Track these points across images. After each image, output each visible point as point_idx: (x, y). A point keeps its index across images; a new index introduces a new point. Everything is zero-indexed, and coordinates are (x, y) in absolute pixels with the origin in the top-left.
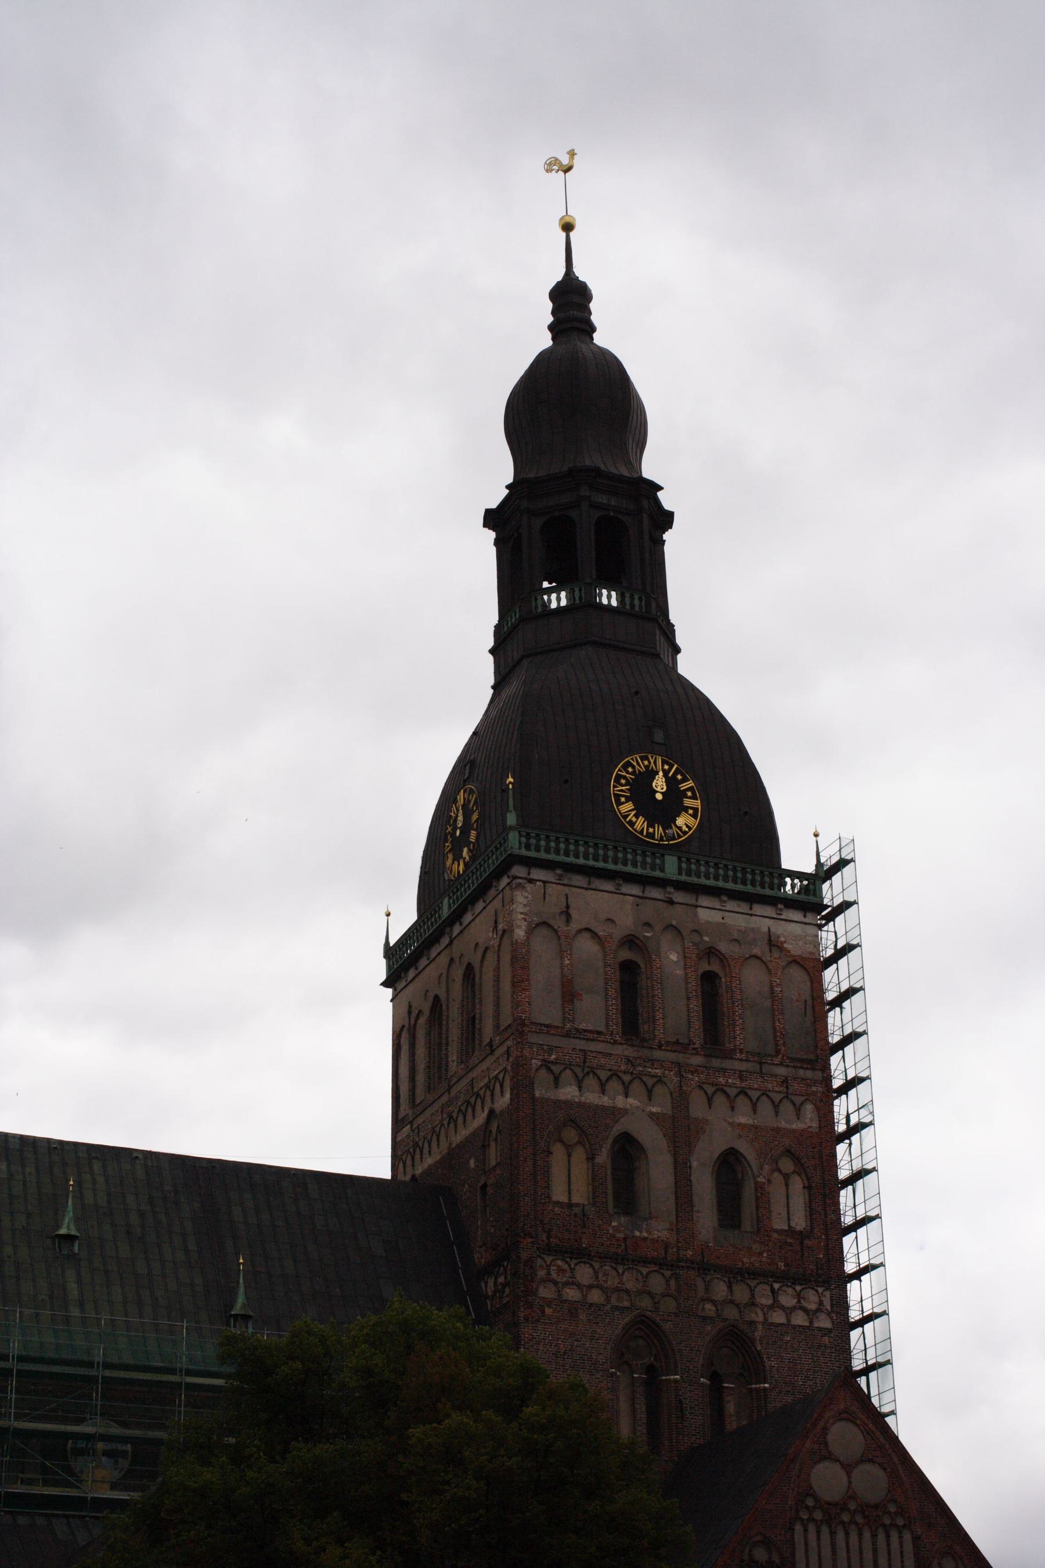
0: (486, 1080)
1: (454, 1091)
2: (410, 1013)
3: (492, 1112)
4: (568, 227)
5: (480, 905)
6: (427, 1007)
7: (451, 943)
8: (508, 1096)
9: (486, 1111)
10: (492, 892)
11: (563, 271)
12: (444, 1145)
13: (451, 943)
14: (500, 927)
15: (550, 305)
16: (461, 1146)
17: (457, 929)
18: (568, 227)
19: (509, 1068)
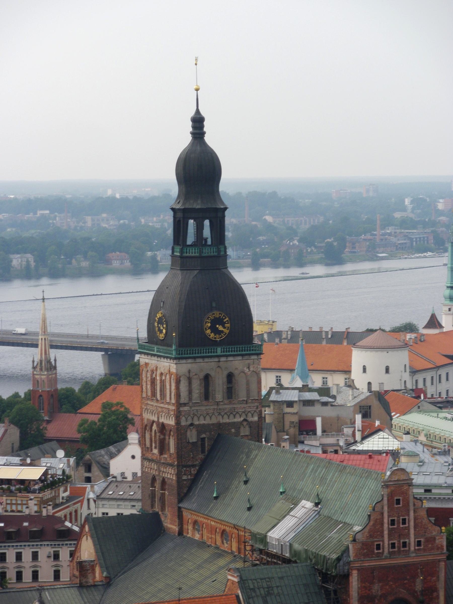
0: (243, 410)
1: (220, 407)
2: (189, 371)
3: (245, 420)
4: (197, 90)
5: (240, 358)
6: (202, 375)
7: (219, 361)
8: (256, 418)
9: (242, 419)
10: (246, 357)
11: (196, 108)
12: (214, 421)
13: (219, 361)
14: (252, 369)
15: (205, 129)
16: (229, 424)
17: (223, 359)
18: (197, 90)
19: (257, 411)
